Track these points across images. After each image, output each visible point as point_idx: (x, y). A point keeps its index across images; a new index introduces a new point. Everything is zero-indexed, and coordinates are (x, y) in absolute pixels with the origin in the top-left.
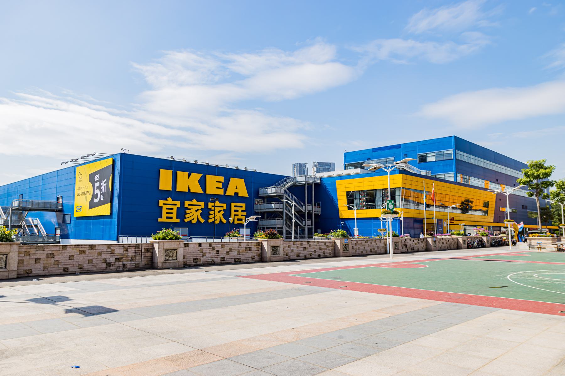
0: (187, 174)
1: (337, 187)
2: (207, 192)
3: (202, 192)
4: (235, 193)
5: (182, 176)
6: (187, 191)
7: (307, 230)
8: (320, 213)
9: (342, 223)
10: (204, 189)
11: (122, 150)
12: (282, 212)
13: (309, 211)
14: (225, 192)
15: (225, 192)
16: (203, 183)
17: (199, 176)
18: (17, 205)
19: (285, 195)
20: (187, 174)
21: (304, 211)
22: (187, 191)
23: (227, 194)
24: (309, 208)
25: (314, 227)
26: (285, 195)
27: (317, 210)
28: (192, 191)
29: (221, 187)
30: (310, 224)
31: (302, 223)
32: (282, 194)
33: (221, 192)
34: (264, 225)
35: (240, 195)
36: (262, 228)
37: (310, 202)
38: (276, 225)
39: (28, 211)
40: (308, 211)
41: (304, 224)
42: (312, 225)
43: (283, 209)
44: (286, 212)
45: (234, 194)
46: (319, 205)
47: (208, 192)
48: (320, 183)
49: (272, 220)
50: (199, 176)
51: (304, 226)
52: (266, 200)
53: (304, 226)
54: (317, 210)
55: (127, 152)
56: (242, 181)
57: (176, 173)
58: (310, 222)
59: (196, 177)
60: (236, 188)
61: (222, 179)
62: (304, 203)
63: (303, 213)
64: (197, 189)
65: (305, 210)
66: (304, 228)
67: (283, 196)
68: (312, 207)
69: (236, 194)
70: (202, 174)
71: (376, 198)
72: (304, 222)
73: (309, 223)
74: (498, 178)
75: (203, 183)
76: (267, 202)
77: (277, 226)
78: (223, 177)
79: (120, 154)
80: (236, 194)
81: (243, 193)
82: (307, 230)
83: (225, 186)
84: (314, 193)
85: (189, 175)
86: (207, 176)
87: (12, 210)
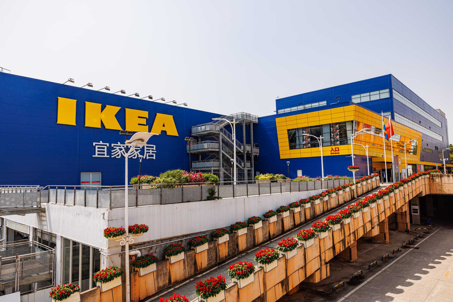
0: (100, 105)
1: (277, 125)
3: (120, 129)
4: (162, 131)
6: (99, 126)
7: (246, 173)
8: (259, 154)
9: (288, 163)
12: (218, 153)
13: (248, 151)
17: (118, 109)
19: (221, 133)
20: (100, 105)
21: (242, 152)
22: (99, 126)
24: (248, 148)
25: (253, 168)
26: (221, 133)
27: (256, 151)
28: (106, 128)
29: (146, 124)
30: (249, 166)
31: (241, 165)
32: (218, 132)
34: (198, 168)
35: (168, 134)
36: (196, 171)
37: (248, 142)
38: (211, 167)
40: (246, 152)
41: (243, 166)
42: (251, 167)
43: (219, 148)
44: (222, 153)
45: (161, 133)
46: (257, 146)
48: (257, 123)
49: (207, 161)
50: (118, 109)
51: (243, 167)
52: (200, 140)
53: (243, 167)
54: (256, 151)
56: (170, 118)
58: (250, 163)
59: (113, 110)
60: (164, 126)
61: (145, 114)
62: (242, 142)
63: (242, 154)
65: (244, 150)
66: (243, 171)
67: (218, 134)
68: (251, 147)
69: (164, 132)
70: (120, 108)
71: (322, 134)
72: (243, 163)
73: (248, 164)
74: (420, 121)
76: (201, 141)
77: (213, 169)
80: (164, 132)
81: (172, 131)
82: (246, 173)
84: (252, 131)
85: (103, 109)
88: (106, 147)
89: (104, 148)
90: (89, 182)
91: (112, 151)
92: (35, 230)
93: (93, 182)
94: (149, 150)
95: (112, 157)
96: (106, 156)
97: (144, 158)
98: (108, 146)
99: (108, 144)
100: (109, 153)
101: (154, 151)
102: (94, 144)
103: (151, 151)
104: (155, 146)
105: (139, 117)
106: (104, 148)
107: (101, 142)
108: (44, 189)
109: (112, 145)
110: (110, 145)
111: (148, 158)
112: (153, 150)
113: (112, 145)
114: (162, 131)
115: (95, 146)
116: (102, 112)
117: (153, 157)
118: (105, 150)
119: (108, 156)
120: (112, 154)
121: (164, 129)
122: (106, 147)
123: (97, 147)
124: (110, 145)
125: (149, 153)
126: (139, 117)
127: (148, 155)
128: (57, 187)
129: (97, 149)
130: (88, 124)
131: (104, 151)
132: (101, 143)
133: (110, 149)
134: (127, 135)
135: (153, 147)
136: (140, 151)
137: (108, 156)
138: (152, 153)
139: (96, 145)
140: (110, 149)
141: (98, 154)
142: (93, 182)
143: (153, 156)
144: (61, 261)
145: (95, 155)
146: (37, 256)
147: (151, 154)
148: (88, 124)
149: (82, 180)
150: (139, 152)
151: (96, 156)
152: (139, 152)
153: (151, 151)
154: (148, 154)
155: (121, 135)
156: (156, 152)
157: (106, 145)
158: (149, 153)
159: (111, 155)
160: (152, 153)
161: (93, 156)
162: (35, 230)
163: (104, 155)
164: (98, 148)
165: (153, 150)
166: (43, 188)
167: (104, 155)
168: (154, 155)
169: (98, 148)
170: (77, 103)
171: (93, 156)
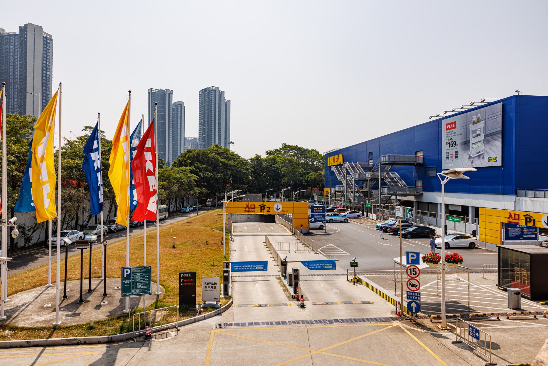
18: (387, 160)
39: (392, 165)
55: (520, 94)
79: (515, 99)
87: (381, 164)
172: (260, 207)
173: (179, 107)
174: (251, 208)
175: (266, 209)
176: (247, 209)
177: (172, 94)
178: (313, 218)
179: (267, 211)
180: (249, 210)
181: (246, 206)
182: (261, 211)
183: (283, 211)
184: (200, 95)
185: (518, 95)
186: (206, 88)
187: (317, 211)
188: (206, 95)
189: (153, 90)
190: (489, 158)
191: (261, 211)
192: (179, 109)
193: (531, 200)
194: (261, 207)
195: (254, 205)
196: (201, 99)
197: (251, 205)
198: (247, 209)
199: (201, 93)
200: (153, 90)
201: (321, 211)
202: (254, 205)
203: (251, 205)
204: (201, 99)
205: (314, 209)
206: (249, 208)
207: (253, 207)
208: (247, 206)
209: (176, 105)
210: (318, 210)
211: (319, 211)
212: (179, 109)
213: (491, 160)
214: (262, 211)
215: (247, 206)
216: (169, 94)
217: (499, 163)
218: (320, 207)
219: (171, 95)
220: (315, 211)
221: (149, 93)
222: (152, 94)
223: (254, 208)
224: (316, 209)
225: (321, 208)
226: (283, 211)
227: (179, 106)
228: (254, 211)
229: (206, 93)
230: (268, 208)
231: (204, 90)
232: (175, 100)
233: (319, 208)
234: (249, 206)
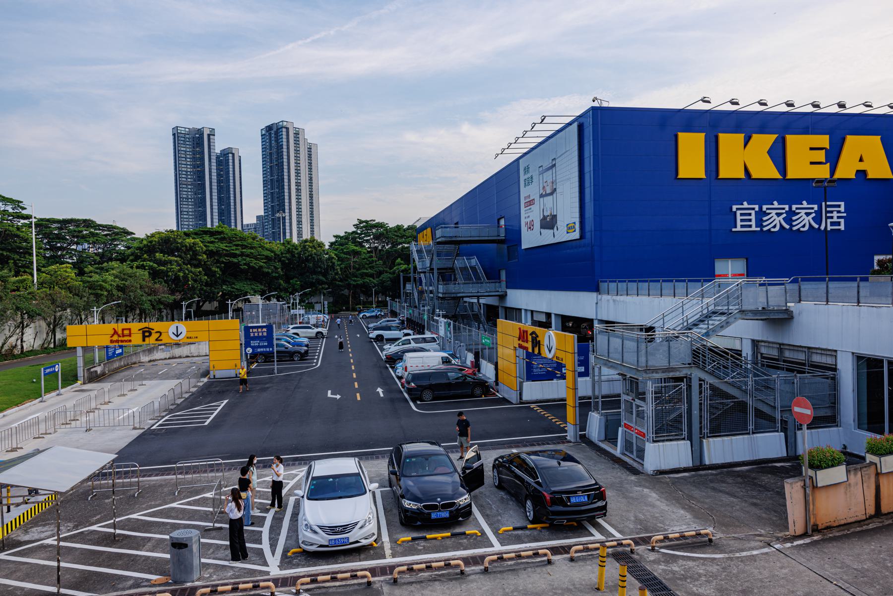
0: (741, 137)
2: (790, 176)
3: (778, 176)
4: (858, 171)
5: (729, 142)
6: (741, 175)
10: (782, 166)
11: (594, 101)
14: (833, 171)
15: (833, 171)
16: (778, 154)
17: (770, 139)
20: (741, 137)
22: (741, 175)
23: (837, 176)
28: (754, 176)
29: (824, 161)
33: (823, 172)
35: (870, 176)
45: (855, 176)
47: (793, 173)
50: (770, 139)
55: (605, 105)
56: (875, 141)
57: (717, 138)
59: (764, 141)
60: (861, 160)
61: (824, 141)
64: (765, 169)
69: (862, 173)
75: (778, 154)
78: (828, 136)
80: (862, 173)
83: (833, 156)
86: (789, 138)
88: (753, 212)
89: (750, 214)
90: (726, 276)
91: (765, 219)
92: (755, 343)
93: (734, 275)
94: (832, 212)
95: (765, 229)
96: (754, 228)
97: (823, 228)
98: (757, 209)
99: (757, 207)
100: (759, 223)
101: (842, 213)
102: (734, 208)
103: (835, 215)
104: (842, 204)
105: (811, 149)
106: (750, 214)
107: (745, 203)
108: (790, 283)
109: (764, 208)
110: (761, 208)
111: (829, 228)
112: (839, 212)
113: (764, 208)
114: (858, 171)
115: (735, 213)
116: (745, 145)
117: (839, 225)
118: (753, 217)
119: (758, 229)
120: (765, 224)
121: (861, 166)
122: (753, 212)
123: (739, 212)
124: (761, 208)
125: (832, 217)
126: (811, 149)
127: (831, 222)
128: (827, 279)
129: (739, 218)
130: (725, 172)
131: (750, 220)
132: (746, 205)
133: (761, 214)
134: (825, 187)
135: (839, 206)
136: (785, 215)
137: (758, 229)
138: (838, 217)
139: (738, 209)
140: (761, 214)
141: (742, 226)
142: (734, 275)
143: (839, 224)
144: (853, 391)
145: (736, 227)
146: (581, 393)
147: (835, 219)
148: (725, 172)
149: (716, 273)
150: (813, 218)
151: (739, 229)
152: (813, 218)
153: (835, 215)
154: (829, 221)
155: (815, 187)
156: (845, 215)
157: (753, 209)
158: (832, 217)
159: (762, 226)
160: (838, 217)
161: (734, 230)
162: (755, 343)
163: (750, 226)
164: (742, 215)
165: (839, 212)
166: (787, 281)
167: (750, 226)
168: (842, 221)
169: (742, 215)
170: (706, 136)
171: (734, 230)
172: (141, 332)
173: (231, 158)
174: (123, 336)
175: (155, 336)
176: (115, 338)
177: (214, 135)
178: (248, 349)
179: (157, 340)
180: (120, 339)
181: (112, 332)
182: (144, 340)
183: (188, 338)
184: (262, 135)
185: (601, 107)
186: (272, 124)
187: (256, 335)
188: (273, 135)
189: (181, 129)
190: (567, 225)
191: (144, 340)
192: (231, 161)
193: (614, 301)
194: (144, 332)
195: (130, 329)
196: (264, 143)
197: (123, 330)
198: (115, 338)
199: (264, 132)
200: (181, 129)
201: (265, 334)
202: (130, 329)
203: (123, 330)
204: (264, 143)
205: (251, 330)
206: (119, 336)
207: (126, 332)
208: (115, 332)
209: (225, 155)
210: (258, 332)
211: (260, 334)
212: (231, 161)
213: (570, 229)
214: (147, 339)
215: (115, 332)
216: (209, 135)
217: (576, 235)
218: (262, 327)
219: (211, 137)
220: (252, 335)
221: (174, 135)
222: (178, 137)
223: (130, 335)
224: (255, 330)
225: (265, 330)
226: (188, 338)
227: (230, 155)
228: (130, 341)
229: (272, 132)
230: (159, 334)
231: (269, 128)
232: (219, 147)
233: (260, 330)
234: (120, 332)
